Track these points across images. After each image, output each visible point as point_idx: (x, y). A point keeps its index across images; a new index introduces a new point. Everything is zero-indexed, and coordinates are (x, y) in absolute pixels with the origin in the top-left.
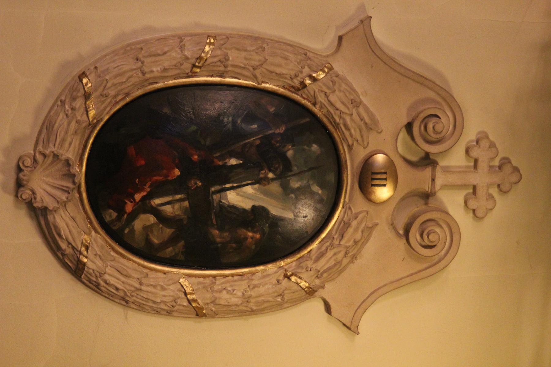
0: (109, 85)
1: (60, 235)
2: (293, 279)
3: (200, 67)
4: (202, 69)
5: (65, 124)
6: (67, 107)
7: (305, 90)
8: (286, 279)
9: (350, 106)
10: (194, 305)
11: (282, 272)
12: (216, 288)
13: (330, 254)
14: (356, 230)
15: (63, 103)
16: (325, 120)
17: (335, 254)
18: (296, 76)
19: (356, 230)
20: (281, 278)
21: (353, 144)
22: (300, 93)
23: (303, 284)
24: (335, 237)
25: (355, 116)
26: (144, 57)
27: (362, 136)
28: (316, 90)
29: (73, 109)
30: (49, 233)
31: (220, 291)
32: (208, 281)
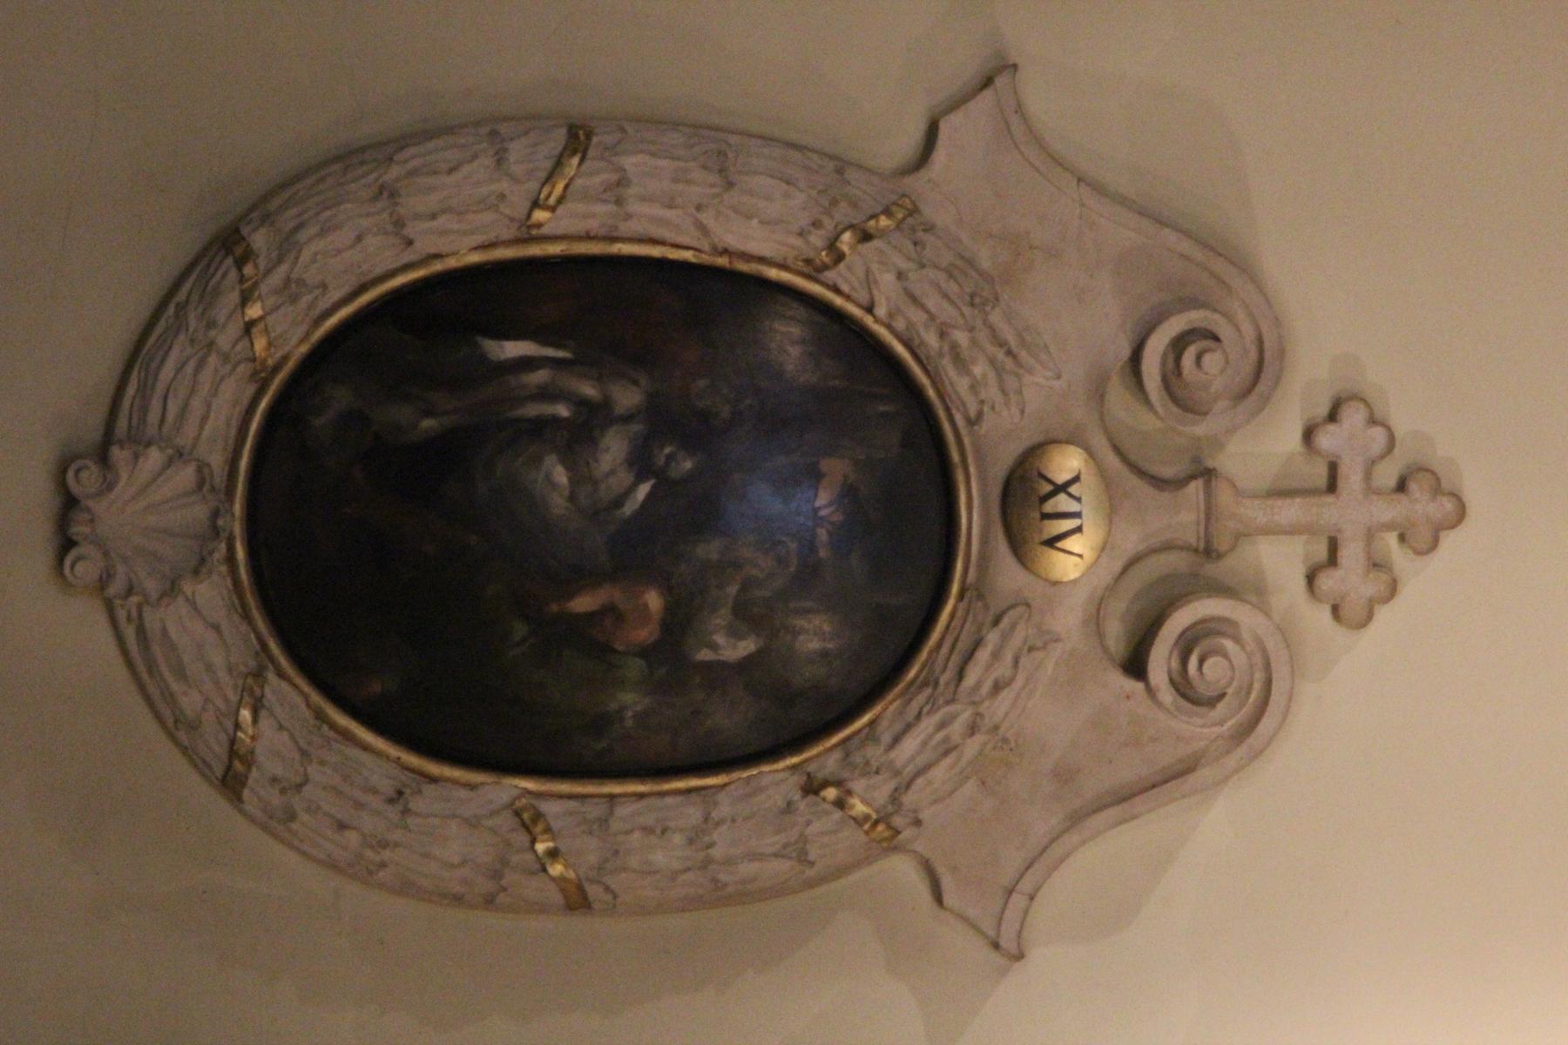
0: (306, 255)
1: (181, 673)
2: (831, 793)
3: (553, 209)
4: (559, 211)
5: (192, 364)
6: (193, 323)
7: (842, 266)
8: (811, 798)
9: (967, 310)
10: (556, 869)
11: (796, 780)
12: (616, 825)
13: (928, 724)
14: (996, 655)
15: (182, 307)
16: (900, 349)
17: (942, 725)
18: (816, 224)
19: (996, 655)
20: (797, 797)
21: (980, 414)
22: (829, 275)
23: (859, 808)
24: (942, 681)
25: (983, 335)
26: (398, 180)
27: (1004, 392)
28: (874, 267)
29: (211, 324)
30: (150, 672)
31: (628, 832)
32: (594, 810)
